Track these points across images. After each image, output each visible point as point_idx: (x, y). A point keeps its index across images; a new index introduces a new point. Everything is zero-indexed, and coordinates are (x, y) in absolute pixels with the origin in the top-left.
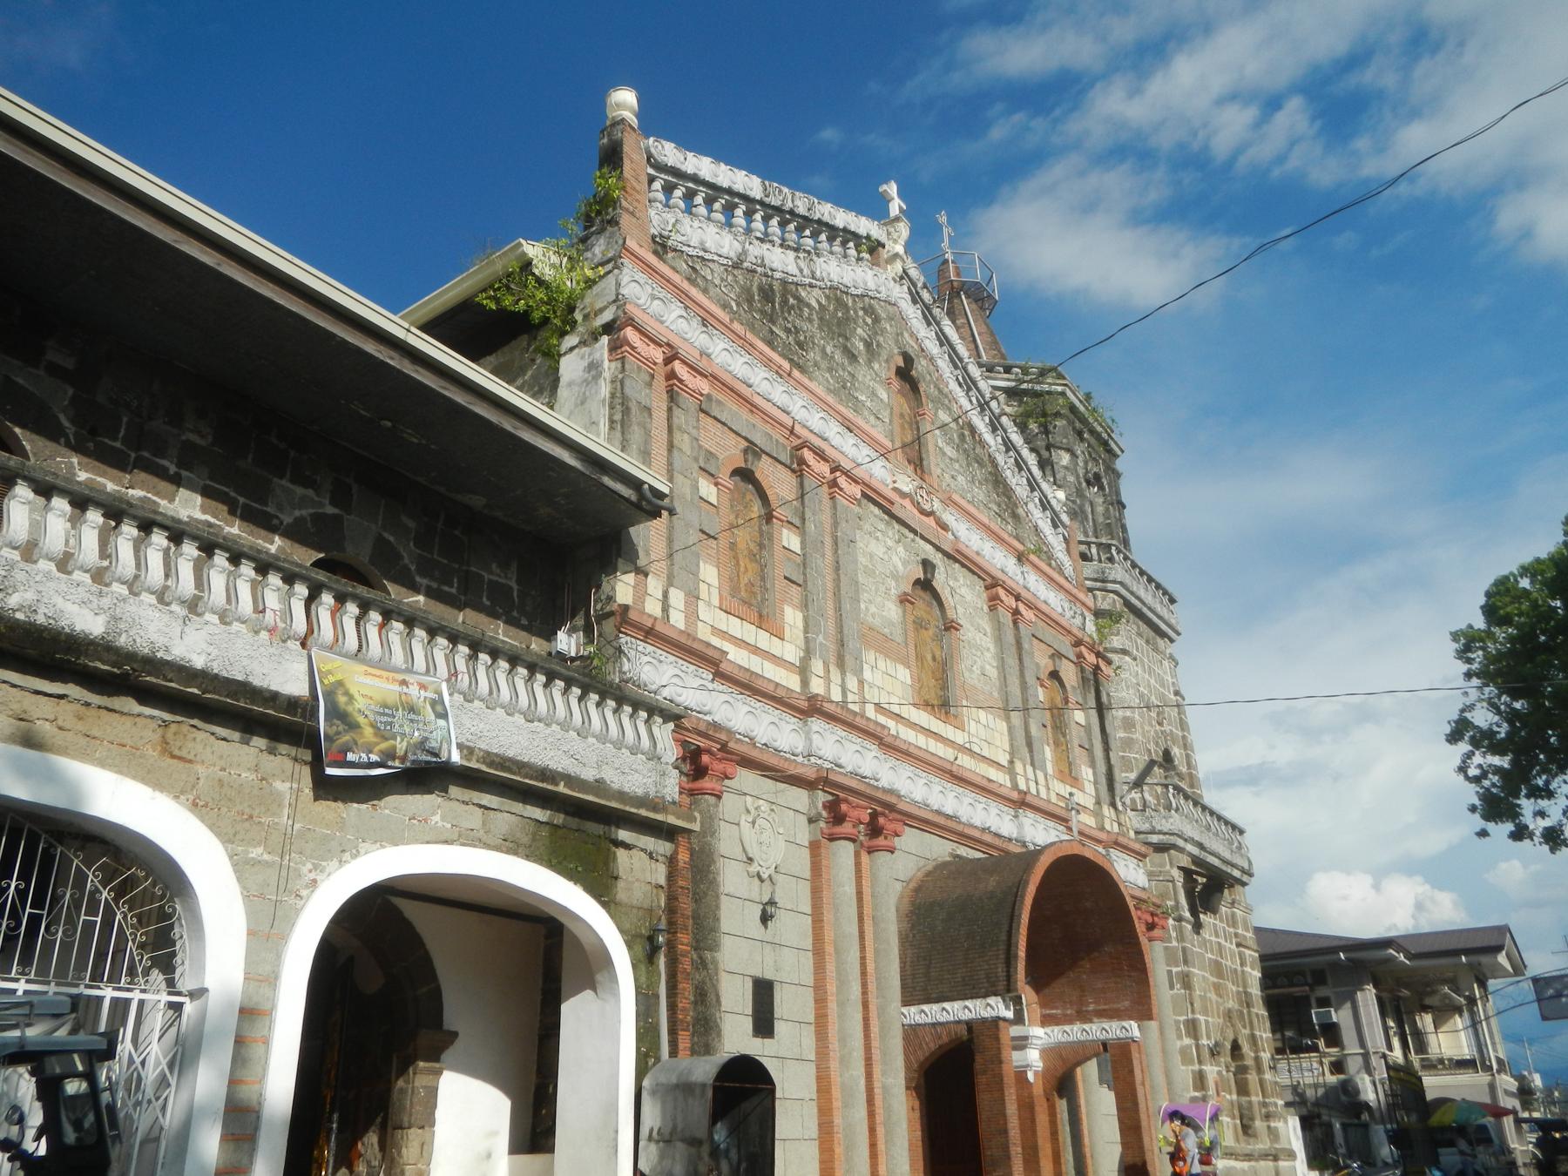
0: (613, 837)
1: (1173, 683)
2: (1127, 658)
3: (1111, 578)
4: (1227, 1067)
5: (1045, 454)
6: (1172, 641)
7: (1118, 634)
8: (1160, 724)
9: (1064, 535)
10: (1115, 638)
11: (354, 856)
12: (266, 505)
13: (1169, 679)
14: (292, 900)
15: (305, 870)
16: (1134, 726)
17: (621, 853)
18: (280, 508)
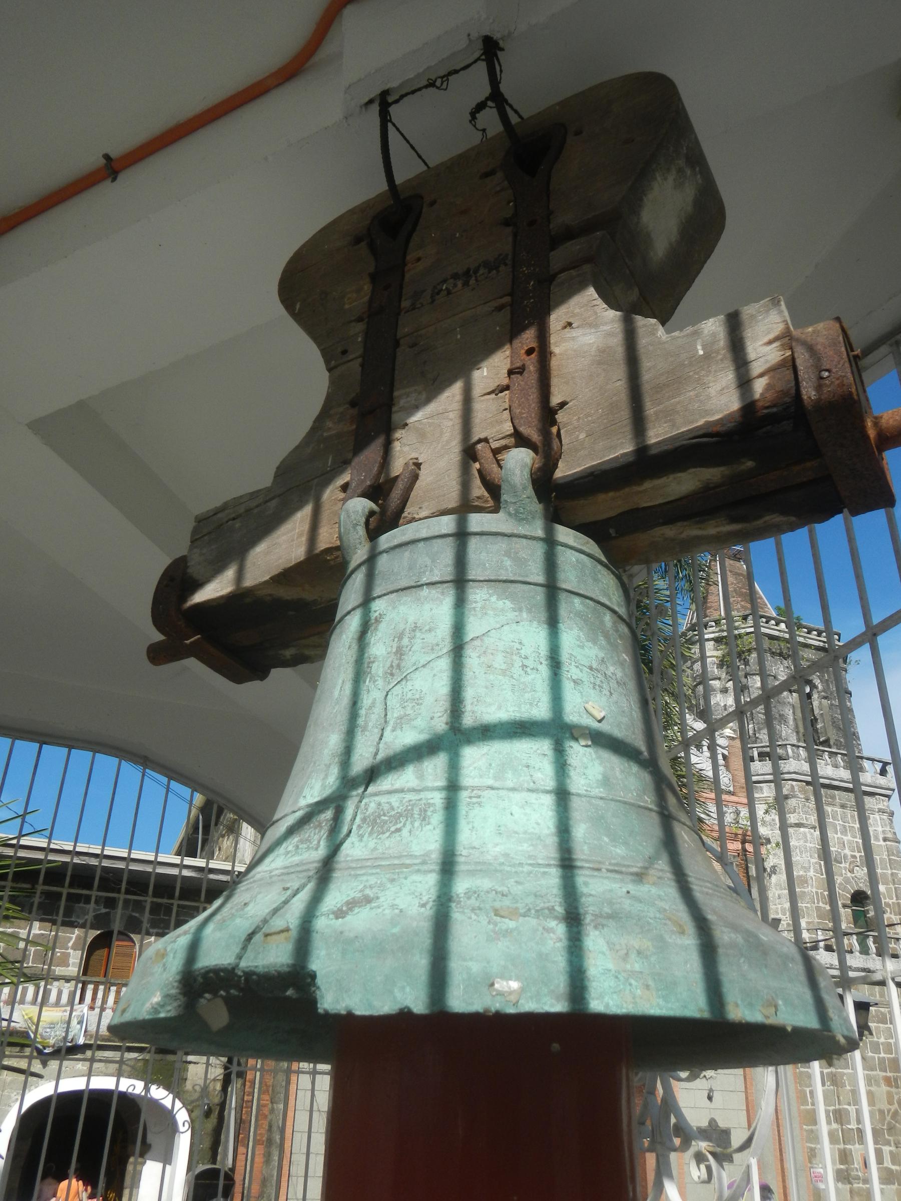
0: (184, 1060)
1: (884, 832)
2: (802, 829)
3: (785, 770)
4: (895, 1144)
5: (744, 680)
6: (889, 797)
7: (795, 812)
8: (852, 871)
9: (723, 755)
10: (792, 815)
11: (36, 1087)
12: (71, 917)
13: (880, 829)
14: (7, 1108)
15: (13, 1095)
16: (806, 882)
17: (191, 1067)
18: (78, 917)
